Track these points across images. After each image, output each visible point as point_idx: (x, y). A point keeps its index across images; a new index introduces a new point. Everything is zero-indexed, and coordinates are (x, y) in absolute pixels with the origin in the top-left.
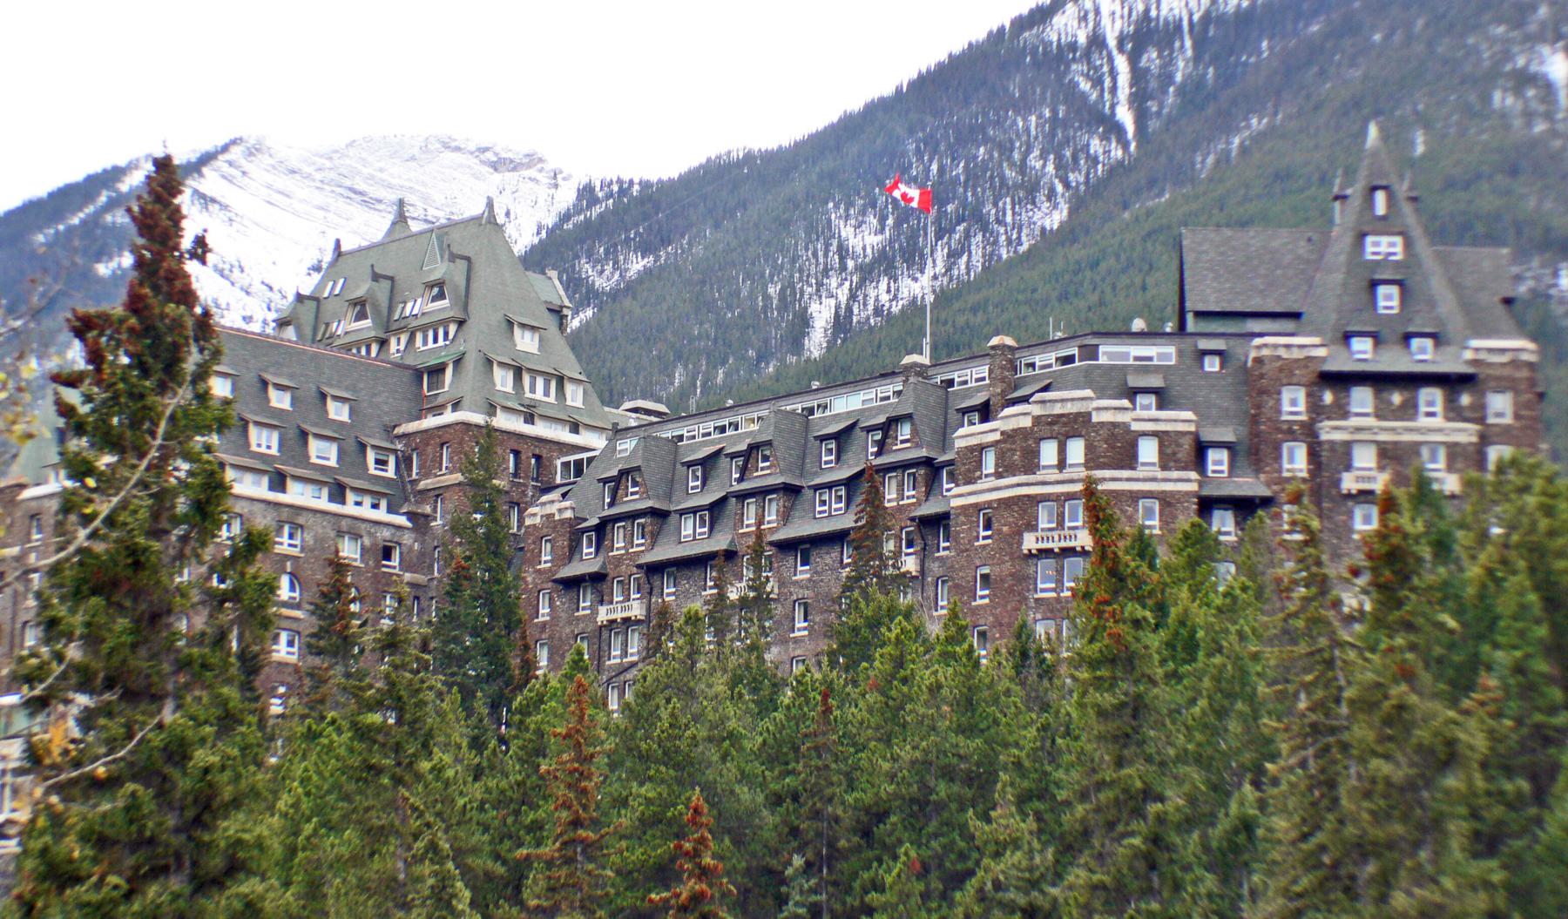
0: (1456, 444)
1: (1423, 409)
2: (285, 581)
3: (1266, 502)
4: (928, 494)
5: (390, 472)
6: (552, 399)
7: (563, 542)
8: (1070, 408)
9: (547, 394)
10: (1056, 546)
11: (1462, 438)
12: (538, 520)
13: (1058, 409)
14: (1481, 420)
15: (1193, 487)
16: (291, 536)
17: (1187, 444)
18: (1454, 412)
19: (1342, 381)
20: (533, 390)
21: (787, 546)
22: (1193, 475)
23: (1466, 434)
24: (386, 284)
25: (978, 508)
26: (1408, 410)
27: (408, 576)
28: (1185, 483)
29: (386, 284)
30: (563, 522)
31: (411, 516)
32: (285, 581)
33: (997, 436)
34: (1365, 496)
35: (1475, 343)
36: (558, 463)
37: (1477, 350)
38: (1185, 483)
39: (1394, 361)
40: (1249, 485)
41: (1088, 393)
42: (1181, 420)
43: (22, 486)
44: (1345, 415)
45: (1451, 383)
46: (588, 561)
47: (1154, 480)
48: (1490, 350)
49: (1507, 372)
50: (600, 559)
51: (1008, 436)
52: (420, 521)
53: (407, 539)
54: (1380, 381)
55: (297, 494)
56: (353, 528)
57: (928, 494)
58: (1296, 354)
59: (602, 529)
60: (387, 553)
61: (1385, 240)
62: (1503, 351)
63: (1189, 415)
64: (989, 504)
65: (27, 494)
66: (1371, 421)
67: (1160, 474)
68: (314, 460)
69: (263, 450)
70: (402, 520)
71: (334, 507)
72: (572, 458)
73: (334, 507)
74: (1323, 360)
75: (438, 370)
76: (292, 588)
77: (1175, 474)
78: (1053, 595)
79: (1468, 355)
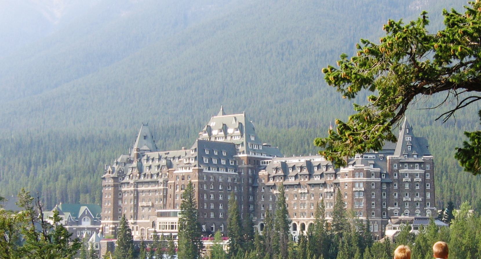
0: (421, 173)
1: (416, 167)
2: (220, 186)
3: (391, 183)
4: (335, 179)
5: (233, 164)
6: (257, 149)
7: (267, 179)
8: (360, 168)
9: (256, 148)
10: (359, 190)
11: (422, 172)
12: (261, 174)
13: (358, 168)
14: (425, 169)
15: (380, 181)
16: (221, 178)
17: (379, 173)
18: (420, 168)
19: (403, 163)
20: (254, 147)
21: (310, 185)
22: (380, 179)
23: (422, 171)
24: (225, 125)
25: (345, 183)
26: (413, 168)
27: (238, 183)
28: (379, 180)
29: (225, 125)
30: (266, 175)
31: (238, 173)
32: (220, 186)
33: (348, 171)
34: (407, 182)
35: (424, 157)
36: (261, 161)
37: (424, 158)
38: (379, 180)
39: (411, 160)
40: (388, 180)
41: (363, 165)
42: (378, 170)
43: (174, 170)
44: (403, 169)
45: (420, 163)
46: (271, 182)
47: (374, 179)
48: (426, 158)
49: (428, 161)
50: (274, 182)
51: (350, 172)
52: (240, 173)
53: (238, 176)
54: (409, 163)
55: (222, 171)
56: (230, 175)
57: (335, 179)
58: (396, 158)
59: (274, 177)
60: (234, 179)
61: (408, 138)
62: (428, 158)
63: (379, 169)
64: (347, 182)
65: (175, 172)
66: (407, 170)
67: (375, 179)
68: (222, 164)
69: (215, 163)
70: (237, 173)
71: (226, 173)
72: (263, 161)
73: (226, 173)
74: (400, 159)
75: (240, 144)
76: (221, 187)
77: (377, 179)
78: (358, 198)
79: (422, 158)
